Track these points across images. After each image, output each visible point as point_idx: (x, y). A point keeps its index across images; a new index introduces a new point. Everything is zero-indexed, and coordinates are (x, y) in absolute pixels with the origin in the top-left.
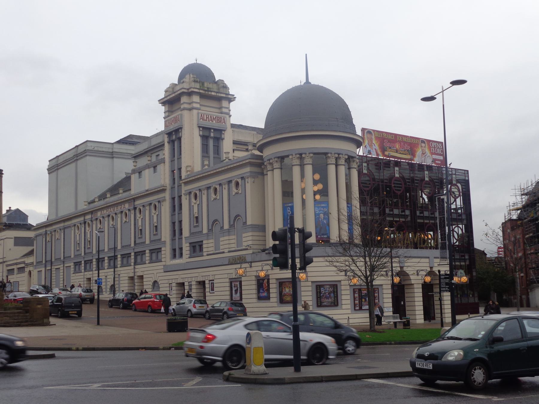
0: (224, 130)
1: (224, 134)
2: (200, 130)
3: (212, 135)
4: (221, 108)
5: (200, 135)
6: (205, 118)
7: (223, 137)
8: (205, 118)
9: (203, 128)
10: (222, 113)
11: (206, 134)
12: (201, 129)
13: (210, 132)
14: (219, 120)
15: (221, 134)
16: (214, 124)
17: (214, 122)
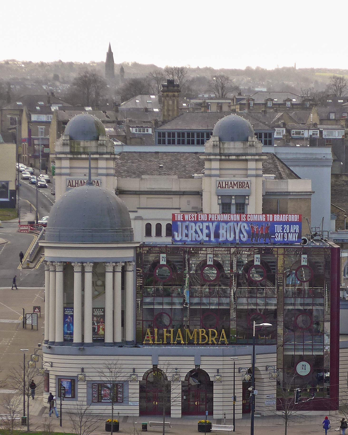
0: (248, 196)
1: (248, 199)
2: (218, 199)
3: (233, 202)
4: (247, 169)
5: (218, 204)
6: (224, 185)
7: (247, 202)
8: (224, 185)
9: (222, 196)
10: (247, 176)
11: (227, 201)
12: (220, 197)
13: (231, 199)
14: (241, 185)
15: (245, 199)
16: (236, 191)
17: (235, 187)
